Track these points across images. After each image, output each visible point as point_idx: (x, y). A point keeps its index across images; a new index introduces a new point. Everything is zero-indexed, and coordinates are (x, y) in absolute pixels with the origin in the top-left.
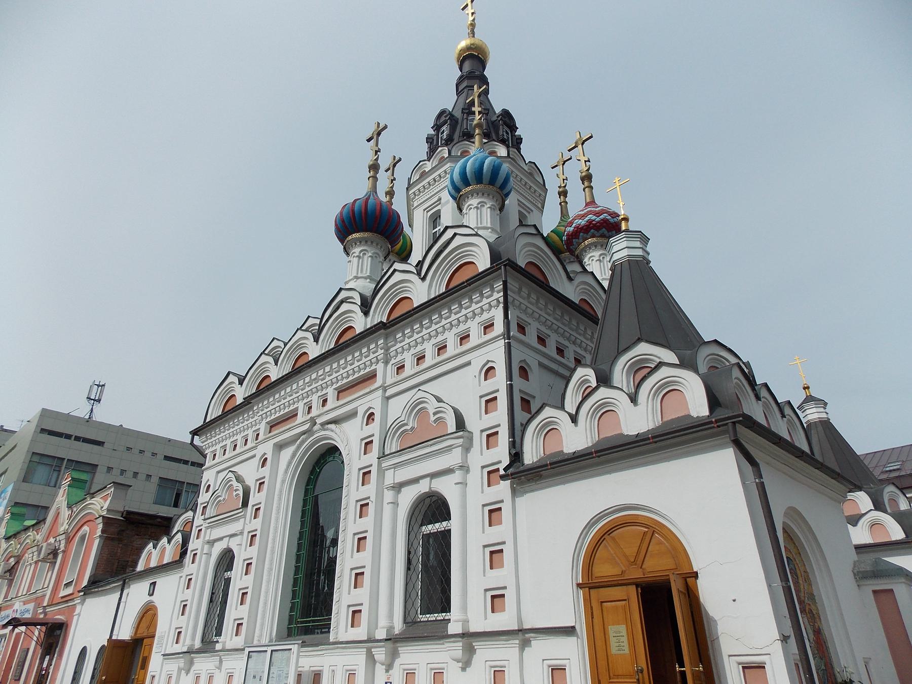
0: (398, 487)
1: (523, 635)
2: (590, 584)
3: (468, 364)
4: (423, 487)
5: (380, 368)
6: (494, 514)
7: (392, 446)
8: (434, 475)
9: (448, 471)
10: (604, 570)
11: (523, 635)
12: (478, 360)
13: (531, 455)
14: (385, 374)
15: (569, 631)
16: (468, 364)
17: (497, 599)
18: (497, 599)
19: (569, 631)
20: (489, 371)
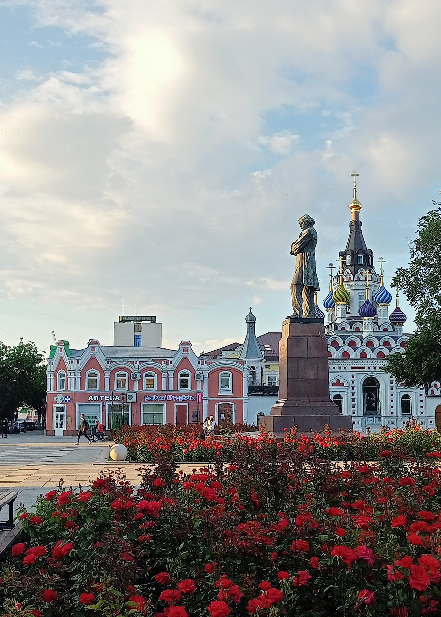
13: (429, 393)
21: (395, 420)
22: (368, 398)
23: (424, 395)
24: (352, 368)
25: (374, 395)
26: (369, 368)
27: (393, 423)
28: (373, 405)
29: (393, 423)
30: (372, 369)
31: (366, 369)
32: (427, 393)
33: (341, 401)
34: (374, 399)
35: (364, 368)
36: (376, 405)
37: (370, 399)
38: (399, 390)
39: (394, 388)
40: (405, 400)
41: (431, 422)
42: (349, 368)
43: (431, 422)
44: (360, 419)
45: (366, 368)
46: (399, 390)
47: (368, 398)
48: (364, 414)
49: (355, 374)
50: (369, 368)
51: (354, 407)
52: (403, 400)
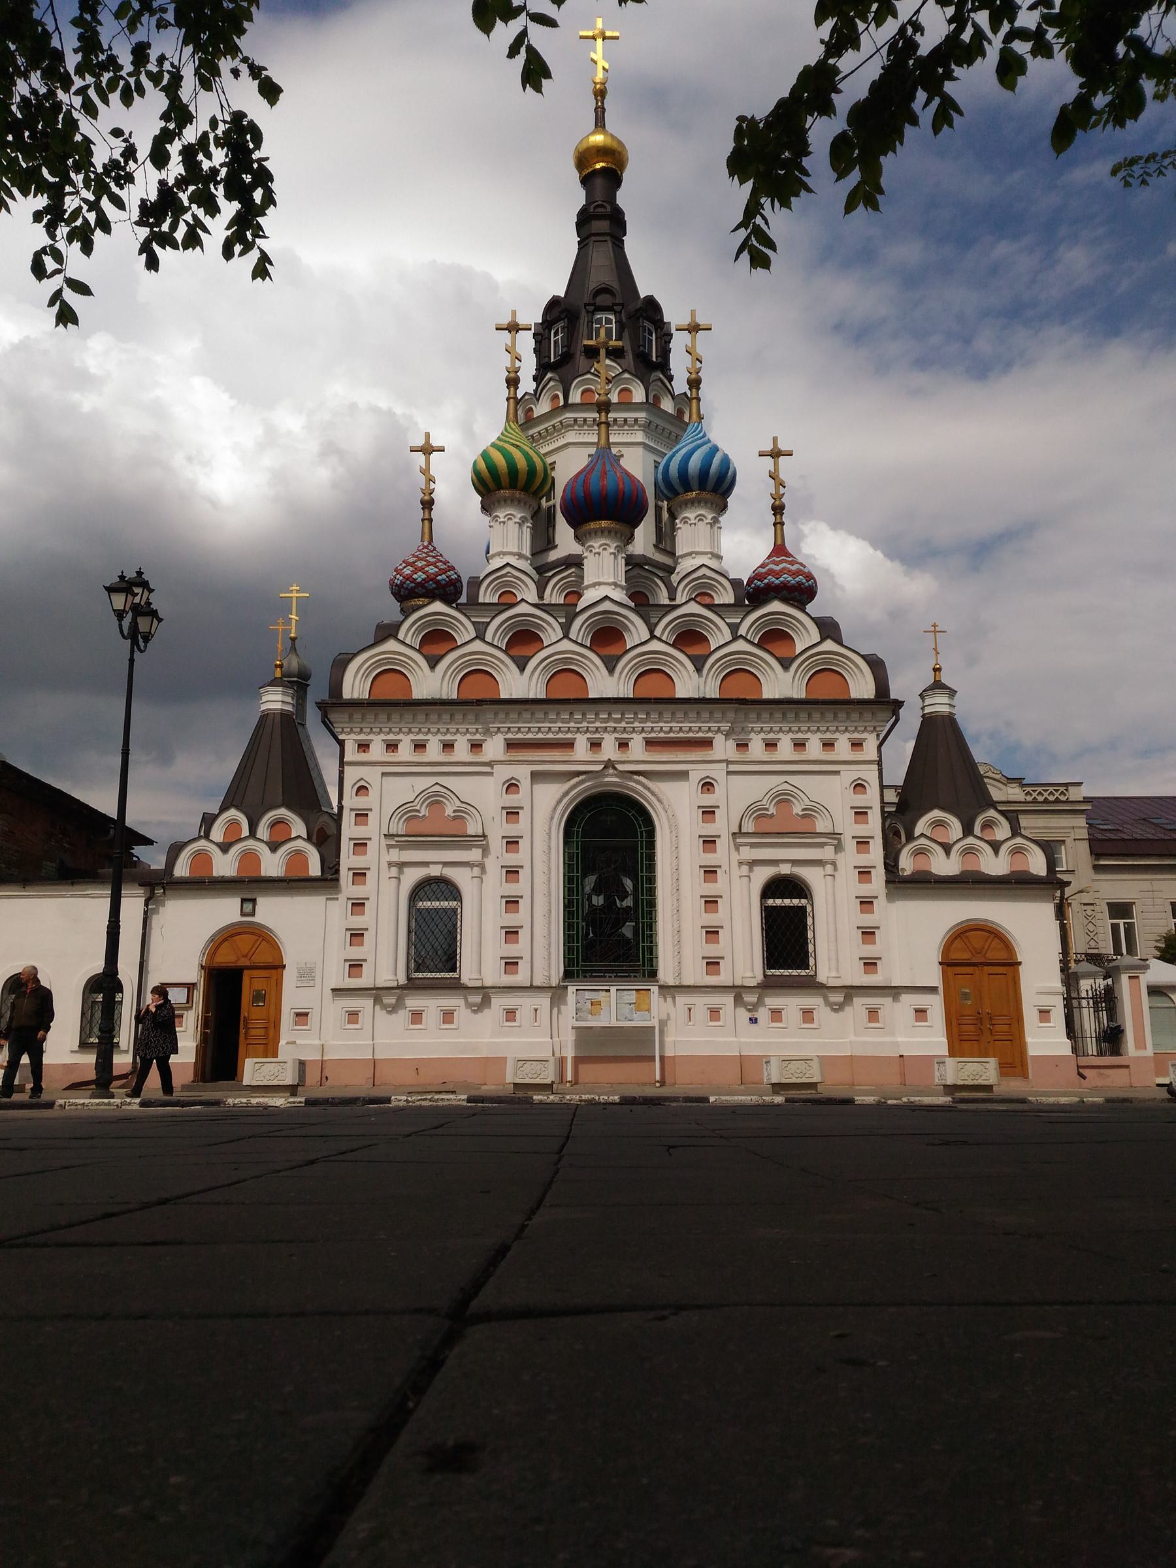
0: (753, 864)
1: (894, 991)
2: (946, 963)
3: (837, 773)
4: (785, 869)
5: (719, 740)
6: (866, 903)
7: (748, 827)
8: (795, 862)
9: (819, 863)
10: (956, 956)
11: (894, 991)
12: (849, 774)
14: (723, 747)
15: (932, 990)
16: (837, 773)
17: (870, 964)
18: (870, 964)
19: (932, 990)
20: (859, 787)
21: (726, 1001)
22: (599, 901)
23: (879, 875)
24: (511, 745)
25: (629, 884)
26: (595, 745)
27: (714, 1013)
28: (627, 930)
29: (714, 1013)
30: (609, 750)
31: (582, 749)
32: (891, 865)
33: (454, 911)
34: (628, 902)
35: (569, 745)
36: (636, 931)
37: (610, 904)
38: (748, 854)
39: (722, 844)
40: (779, 902)
41: (921, 1013)
42: (494, 747)
43: (921, 1013)
44: (544, 1001)
45: (581, 742)
46: (748, 854)
47: (599, 901)
48: (568, 975)
49: (522, 773)
50: (595, 745)
51: (511, 933)
52: (770, 902)
